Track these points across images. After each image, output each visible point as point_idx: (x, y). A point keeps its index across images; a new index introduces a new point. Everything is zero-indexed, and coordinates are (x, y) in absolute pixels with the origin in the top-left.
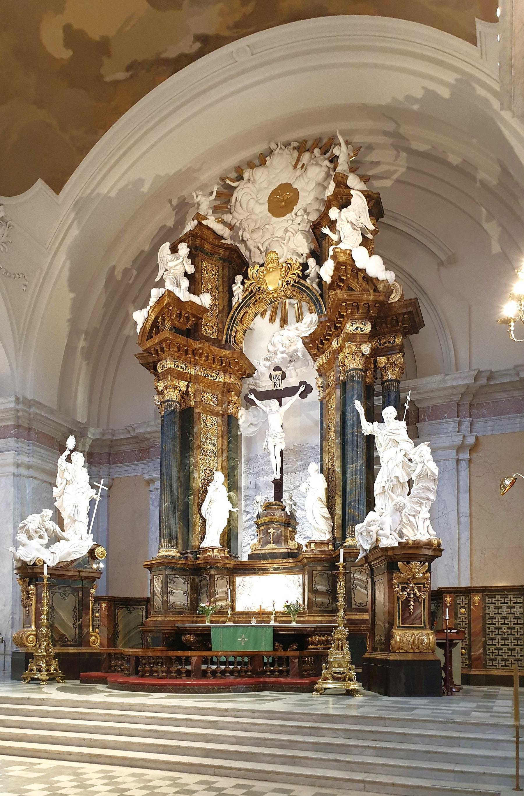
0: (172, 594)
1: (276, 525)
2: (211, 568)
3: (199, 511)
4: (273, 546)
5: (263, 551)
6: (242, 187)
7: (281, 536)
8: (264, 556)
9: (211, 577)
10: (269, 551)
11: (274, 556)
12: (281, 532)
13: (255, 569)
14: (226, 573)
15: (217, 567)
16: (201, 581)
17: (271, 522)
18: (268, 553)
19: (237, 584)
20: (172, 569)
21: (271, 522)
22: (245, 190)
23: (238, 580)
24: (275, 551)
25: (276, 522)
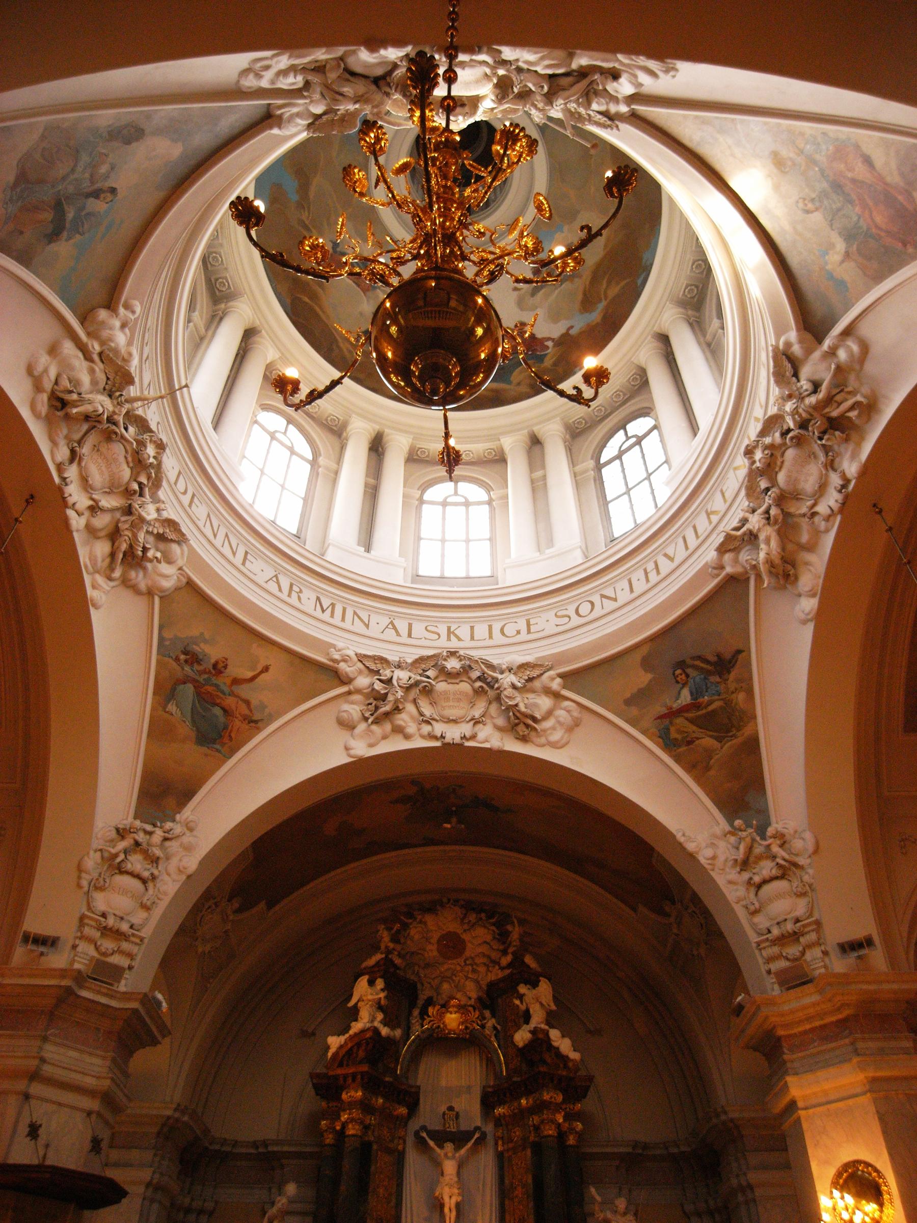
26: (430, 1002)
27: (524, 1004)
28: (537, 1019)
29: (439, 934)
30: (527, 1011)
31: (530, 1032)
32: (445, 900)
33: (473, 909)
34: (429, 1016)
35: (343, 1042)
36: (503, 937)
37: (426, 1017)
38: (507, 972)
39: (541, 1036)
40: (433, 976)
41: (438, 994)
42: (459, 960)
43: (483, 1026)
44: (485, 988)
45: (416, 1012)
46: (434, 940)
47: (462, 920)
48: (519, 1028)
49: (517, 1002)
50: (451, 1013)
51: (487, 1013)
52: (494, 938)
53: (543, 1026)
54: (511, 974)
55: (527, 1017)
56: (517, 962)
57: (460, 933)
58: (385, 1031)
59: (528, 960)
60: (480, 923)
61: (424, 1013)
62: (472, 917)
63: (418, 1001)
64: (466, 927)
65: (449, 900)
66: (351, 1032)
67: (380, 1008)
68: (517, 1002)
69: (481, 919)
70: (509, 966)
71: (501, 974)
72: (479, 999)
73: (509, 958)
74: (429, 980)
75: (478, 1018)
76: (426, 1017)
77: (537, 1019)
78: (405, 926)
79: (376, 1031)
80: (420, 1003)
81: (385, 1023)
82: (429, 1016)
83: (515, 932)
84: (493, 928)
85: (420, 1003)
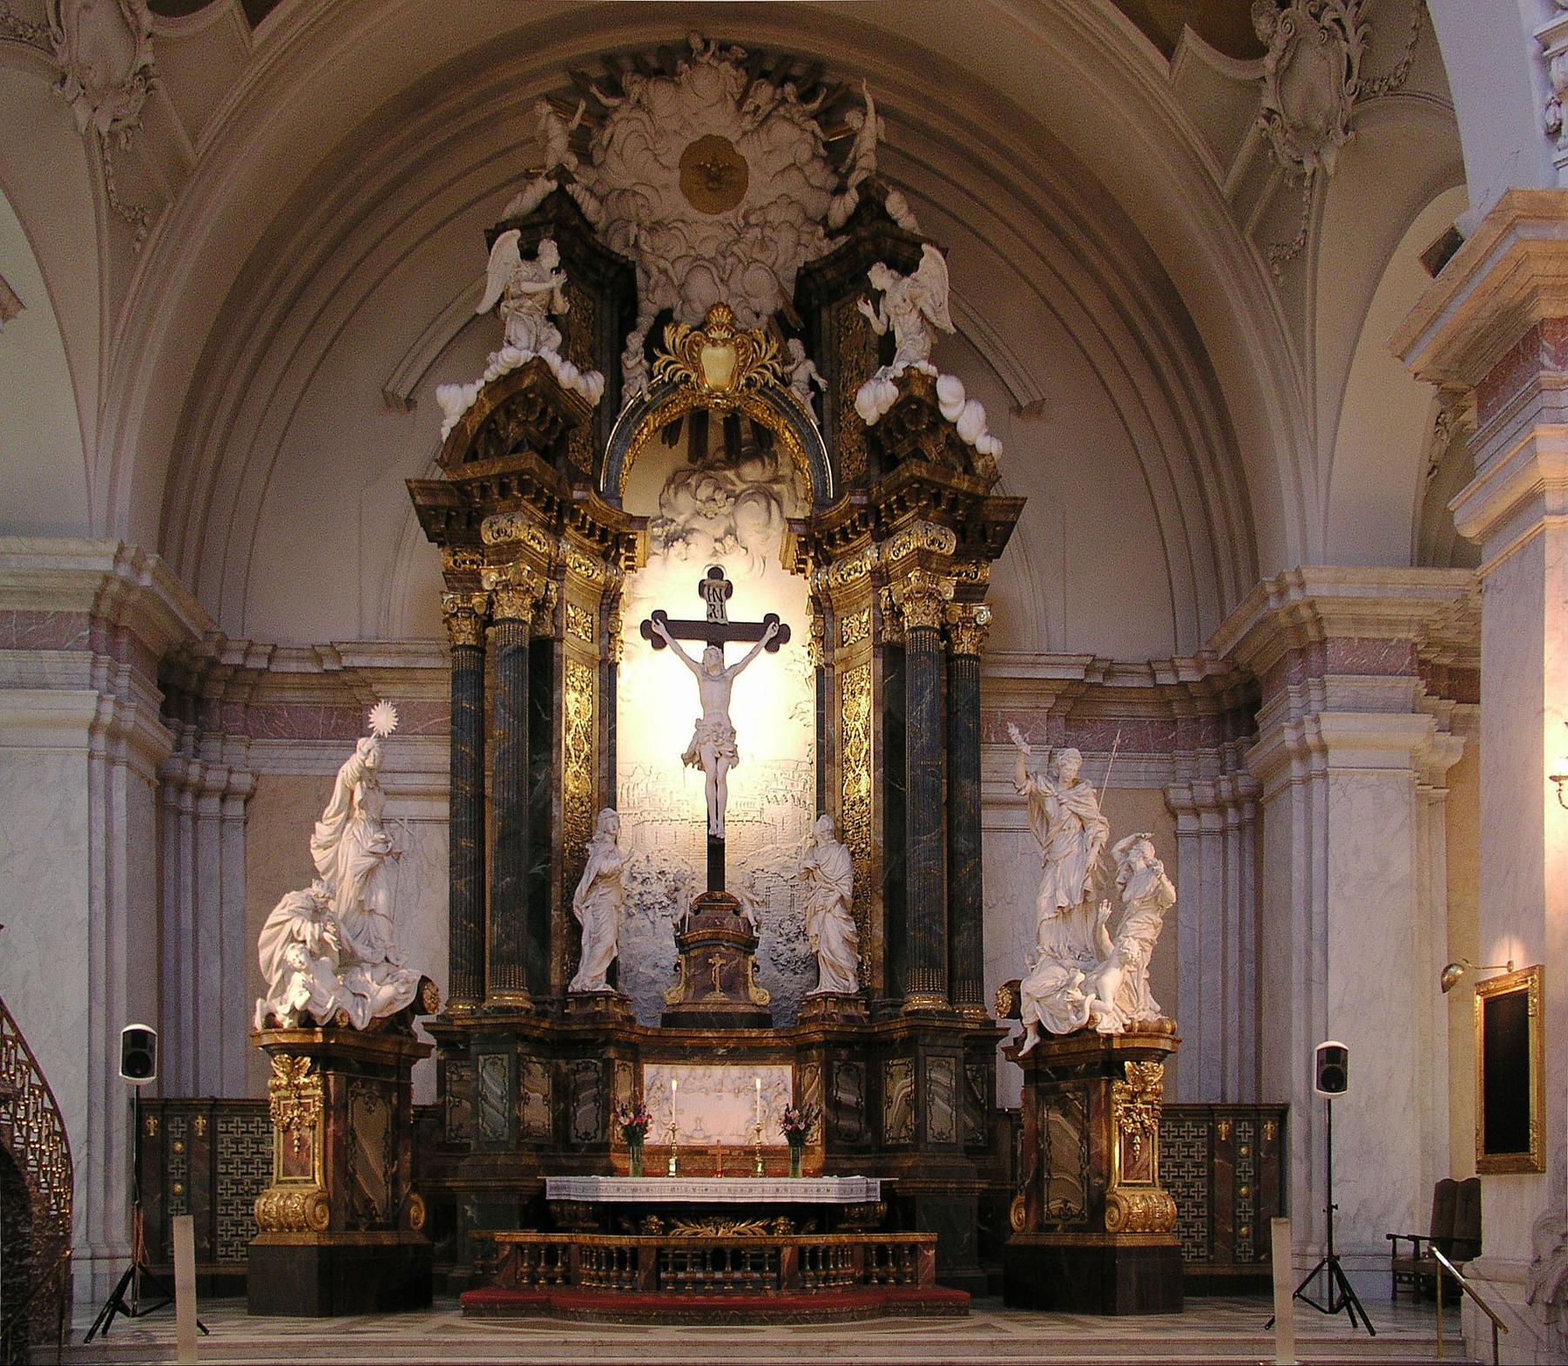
0: (524, 1100)
1: (728, 948)
2: (607, 1043)
3: (568, 895)
4: (718, 996)
5: (701, 1008)
6: (626, 115)
7: (737, 974)
8: (706, 1020)
9: (608, 1064)
10: (715, 1009)
11: (724, 1021)
12: (738, 965)
13: (684, 1048)
14: (629, 1056)
15: (618, 1041)
16: (576, 1072)
17: (716, 940)
18: (714, 1014)
19: (646, 1080)
20: (525, 1039)
21: (716, 940)
22: (634, 125)
23: (649, 1070)
24: (728, 1009)
25: (728, 941)
26: (665, 317)
27: (883, 317)
28: (912, 351)
29: (685, 144)
30: (889, 336)
31: (895, 381)
32: (696, 43)
33: (765, 75)
34: (665, 351)
35: (472, 400)
36: (836, 154)
37: (657, 352)
38: (843, 240)
39: (919, 391)
40: (672, 255)
41: (686, 301)
42: (730, 214)
43: (785, 381)
44: (791, 289)
45: (635, 341)
46: (673, 159)
47: (740, 104)
48: (864, 376)
49: (867, 310)
50: (714, 343)
51: (795, 346)
52: (815, 156)
53: (925, 367)
54: (850, 248)
55: (886, 348)
56: (871, 205)
57: (733, 139)
58: (566, 374)
59: (895, 205)
60: (782, 110)
61: (654, 342)
62: (764, 94)
63: (640, 320)
64: (747, 123)
65: (707, 44)
66: (490, 375)
67: (551, 318)
68: (867, 310)
69: (784, 101)
70: (853, 220)
71: (827, 247)
72: (779, 316)
73: (851, 199)
74: (662, 263)
75: (774, 357)
76: (657, 352)
77: (912, 351)
78: (602, 117)
79: (540, 365)
80: (645, 322)
81: (563, 351)
82: (665, 351)
83: (868, 130)
84: (814, 125)
85: (645, 322)
